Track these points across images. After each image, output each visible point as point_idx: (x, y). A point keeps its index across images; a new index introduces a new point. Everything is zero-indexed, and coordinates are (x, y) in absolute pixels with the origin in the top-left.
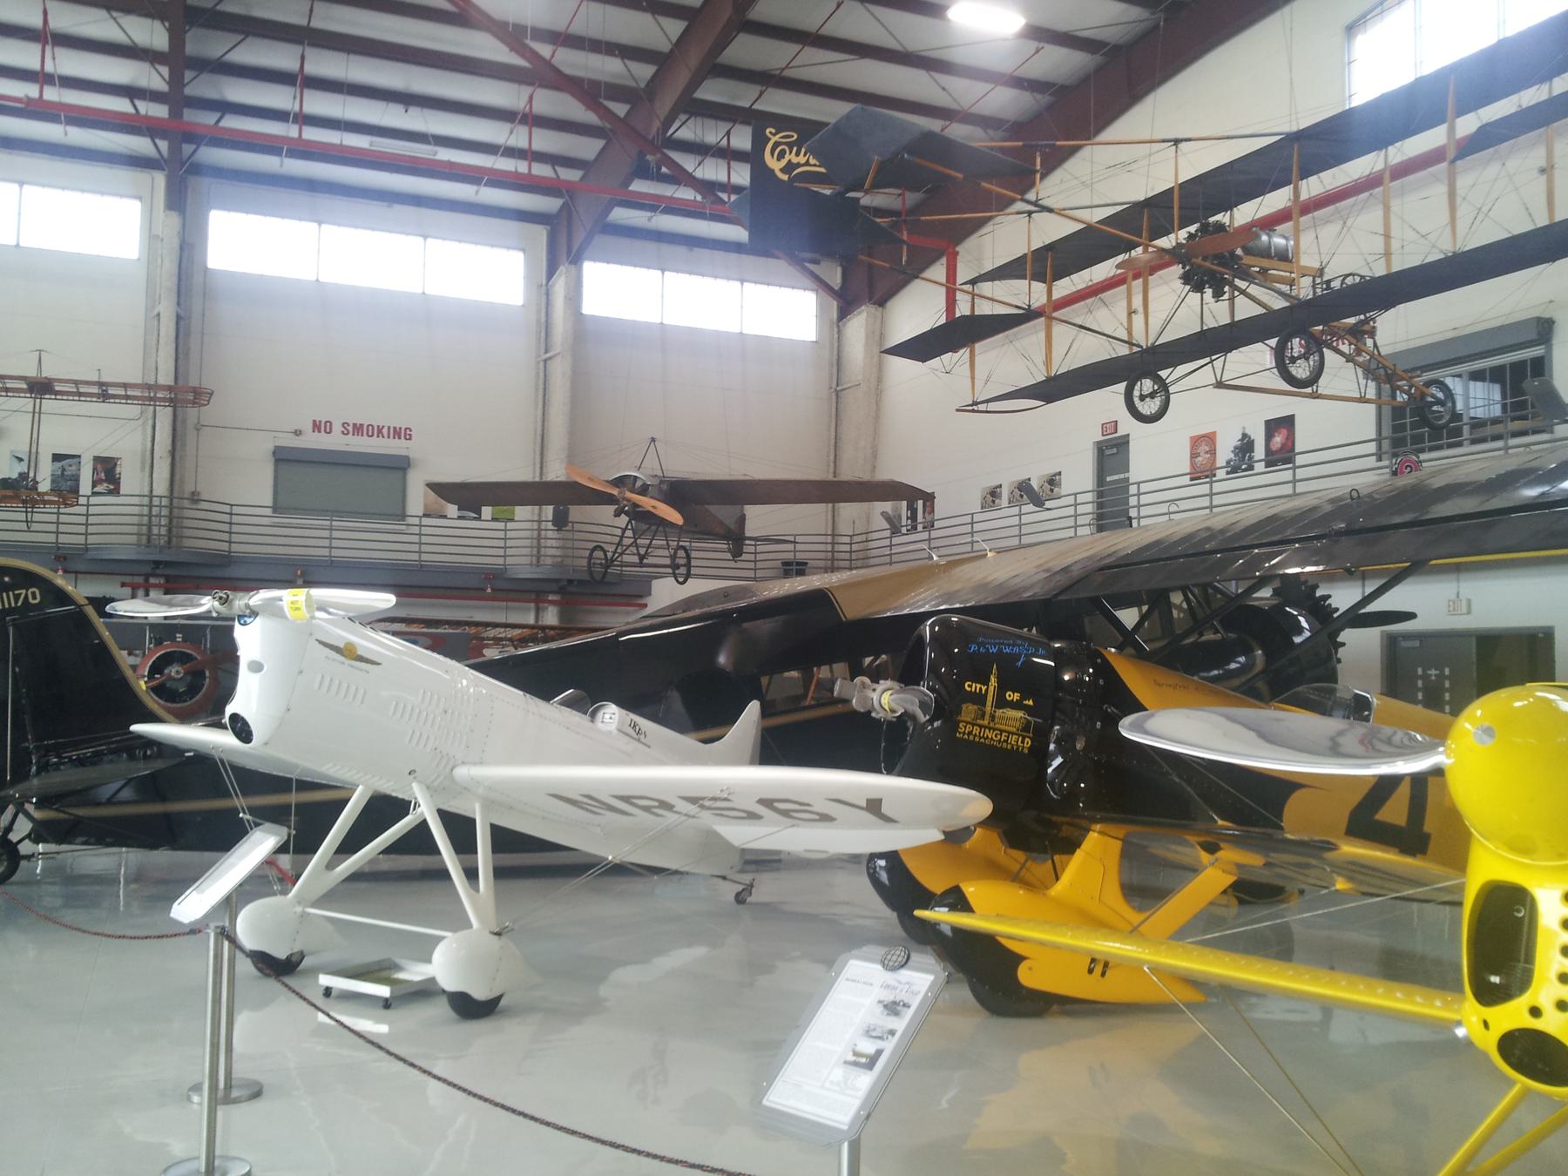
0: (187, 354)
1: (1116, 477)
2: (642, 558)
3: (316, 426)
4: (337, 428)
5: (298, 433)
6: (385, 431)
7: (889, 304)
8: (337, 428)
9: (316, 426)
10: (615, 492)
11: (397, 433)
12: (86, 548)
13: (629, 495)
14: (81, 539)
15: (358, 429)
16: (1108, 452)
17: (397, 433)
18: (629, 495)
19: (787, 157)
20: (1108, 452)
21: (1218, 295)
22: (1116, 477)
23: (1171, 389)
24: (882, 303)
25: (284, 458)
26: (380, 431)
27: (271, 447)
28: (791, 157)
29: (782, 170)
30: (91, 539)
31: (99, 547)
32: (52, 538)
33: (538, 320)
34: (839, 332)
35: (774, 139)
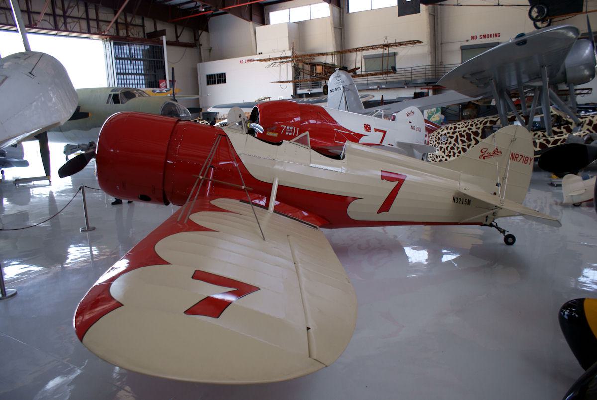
0: (438, 25)
3: (472, 38)
4: (478, 37)
5: (467, 41)
6: (492, 36)
8: (478, 37)
9: (472, 38)
11: (496, 35)
12: (412, 80)
14: (410, 79)
15: (484, 36)
17: (496, 35)
25: (463, 49)
26: (491, 36)
27: (459, 47)
30: (413, 78)
31: (416, 80)
32: (404, 79)
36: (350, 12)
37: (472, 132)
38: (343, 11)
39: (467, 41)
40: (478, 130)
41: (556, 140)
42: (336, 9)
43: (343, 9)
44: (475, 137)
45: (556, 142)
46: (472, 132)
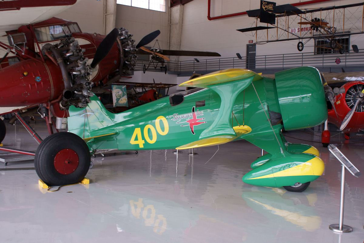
1: (251, 52)
2: (155, 68)
7: (185, 5)
10: (153, 53)
13: (156, 53)
16: (250, 47)
18: (156, 53)
19: (266, 7)
20: (250, 47)
21: (317, 30)
22: (251, 52)
23: (304, 46)
24: (183, 4)
28: (266, 7)
29: (265, 9)
33: (104, 5)
34: (171, 9)
35: (264, 3)
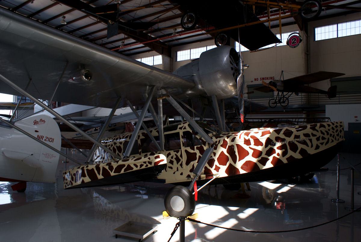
3: (255, 80)
4: (259, 79)
5: (252, 81)
6: (269, 78)
8: (259, 79)
9: (255, 80)
26: (268, 78)
36: (179, 60)
37: (117, 146)
38: (173, 60)
39: (252, 81)
40: (120, 145)
41: (121, 165)
42: (168, 59)
43: (173, 58)
44: (119, 153)
45: (120, 167)
46: (117, 146)
